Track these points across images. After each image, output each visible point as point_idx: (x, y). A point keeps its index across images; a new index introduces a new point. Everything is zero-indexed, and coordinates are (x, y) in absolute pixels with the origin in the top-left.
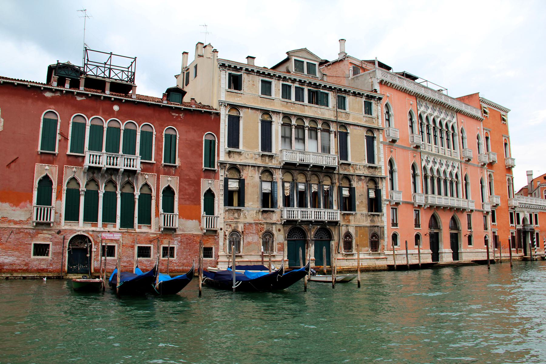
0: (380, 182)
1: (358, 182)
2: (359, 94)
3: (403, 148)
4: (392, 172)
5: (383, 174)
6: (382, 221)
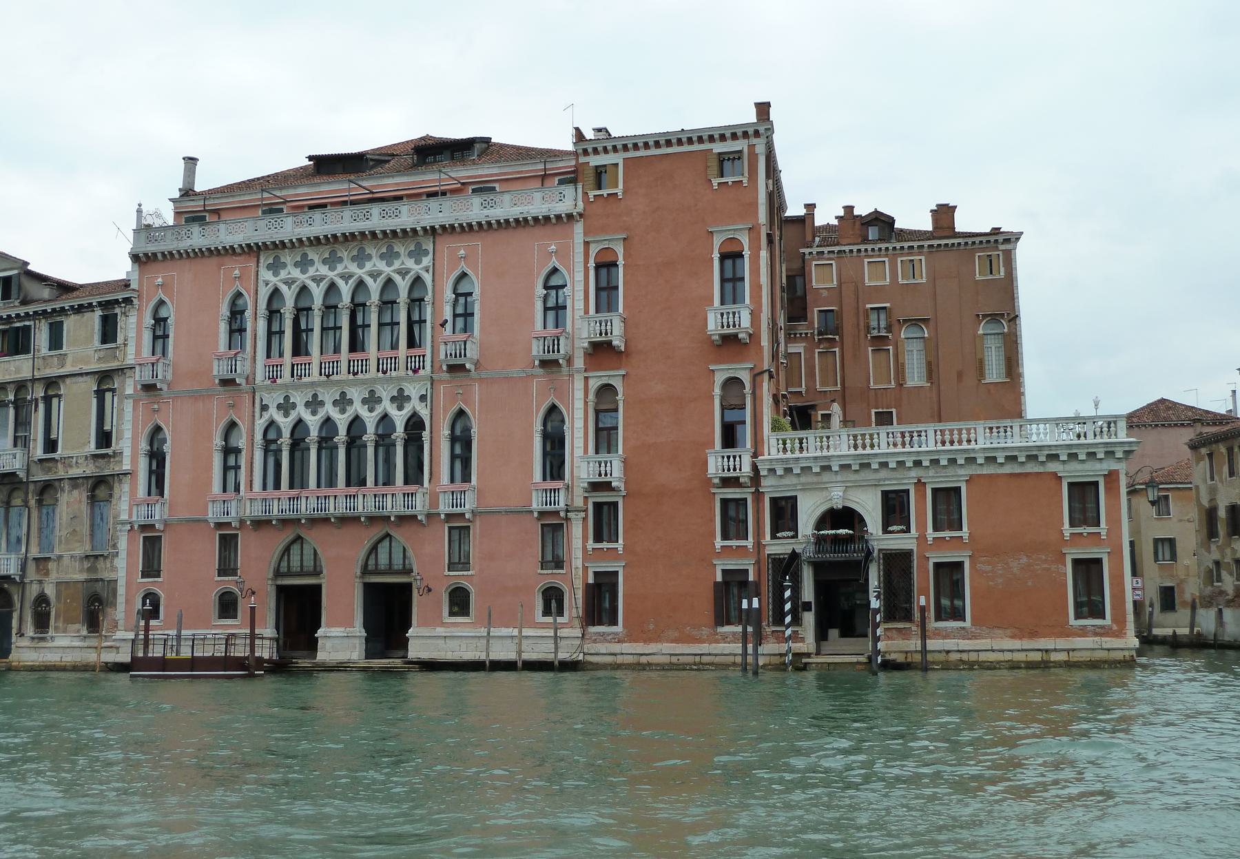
0: (116, 485)
1: (70, 492)
2: (81, 306)
3: (196, 396)
4: (157, 458)
5: (126, 466)
6: (114, 569)
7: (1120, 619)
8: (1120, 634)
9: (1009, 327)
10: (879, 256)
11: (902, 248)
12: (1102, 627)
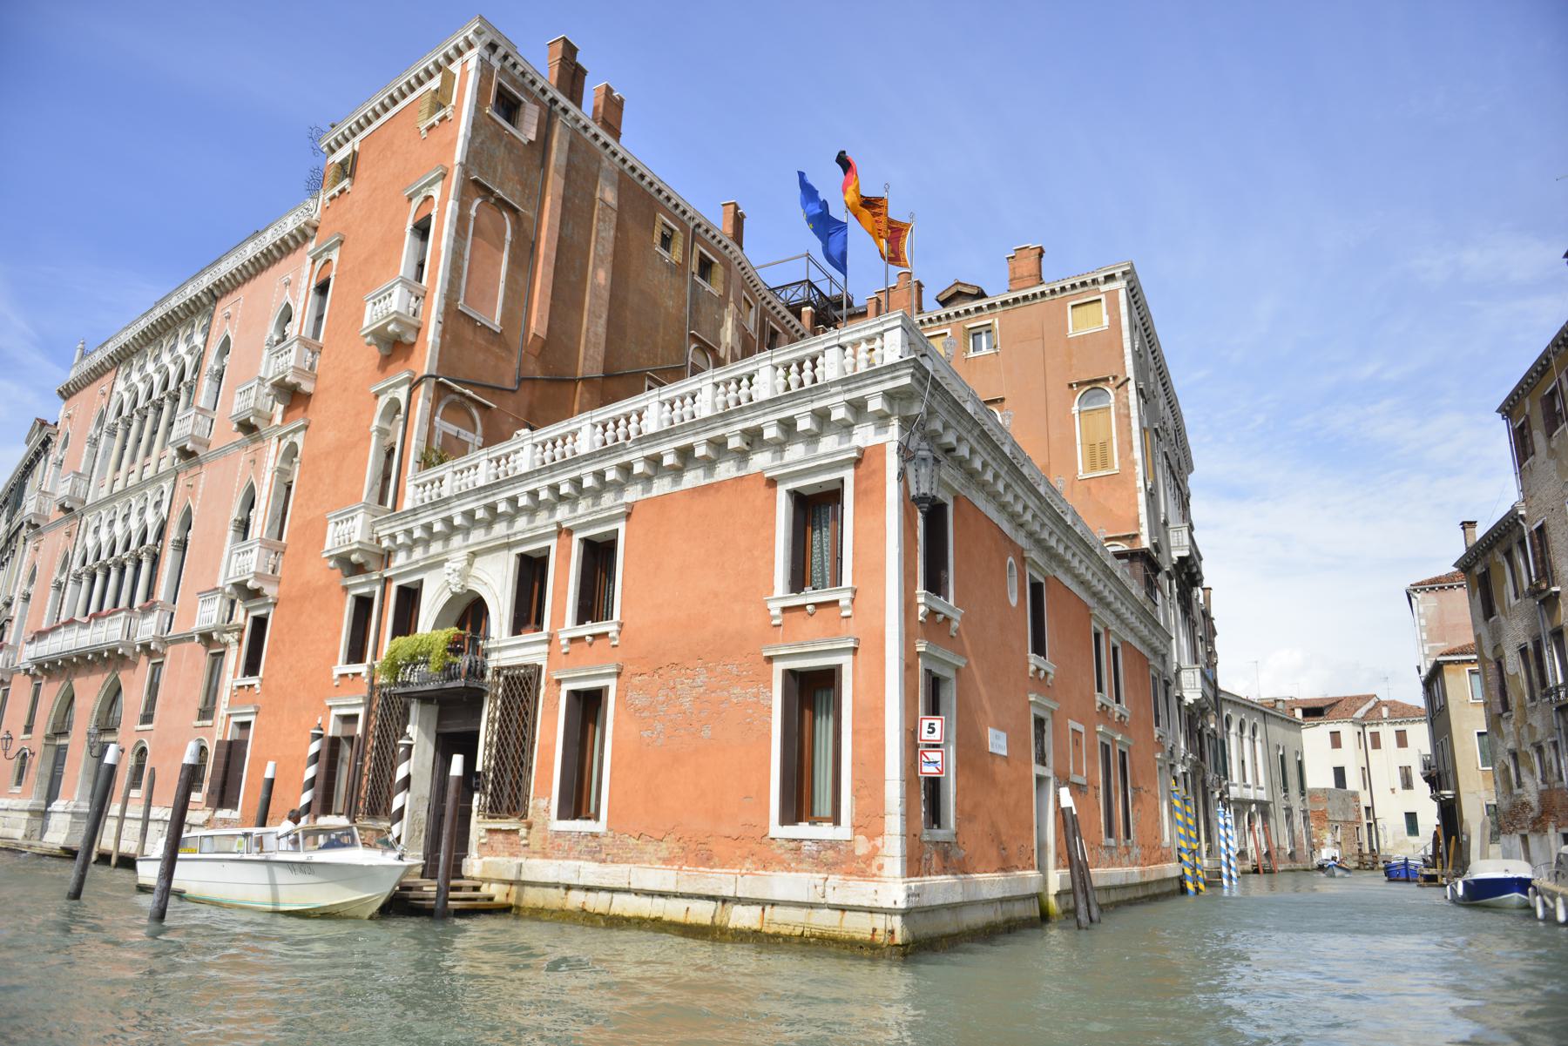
7: (870, 824)
8: (864, 868)
9: (1116, 395)
10: (939, 327)
11: (967, 312)
12: (833, 845)
